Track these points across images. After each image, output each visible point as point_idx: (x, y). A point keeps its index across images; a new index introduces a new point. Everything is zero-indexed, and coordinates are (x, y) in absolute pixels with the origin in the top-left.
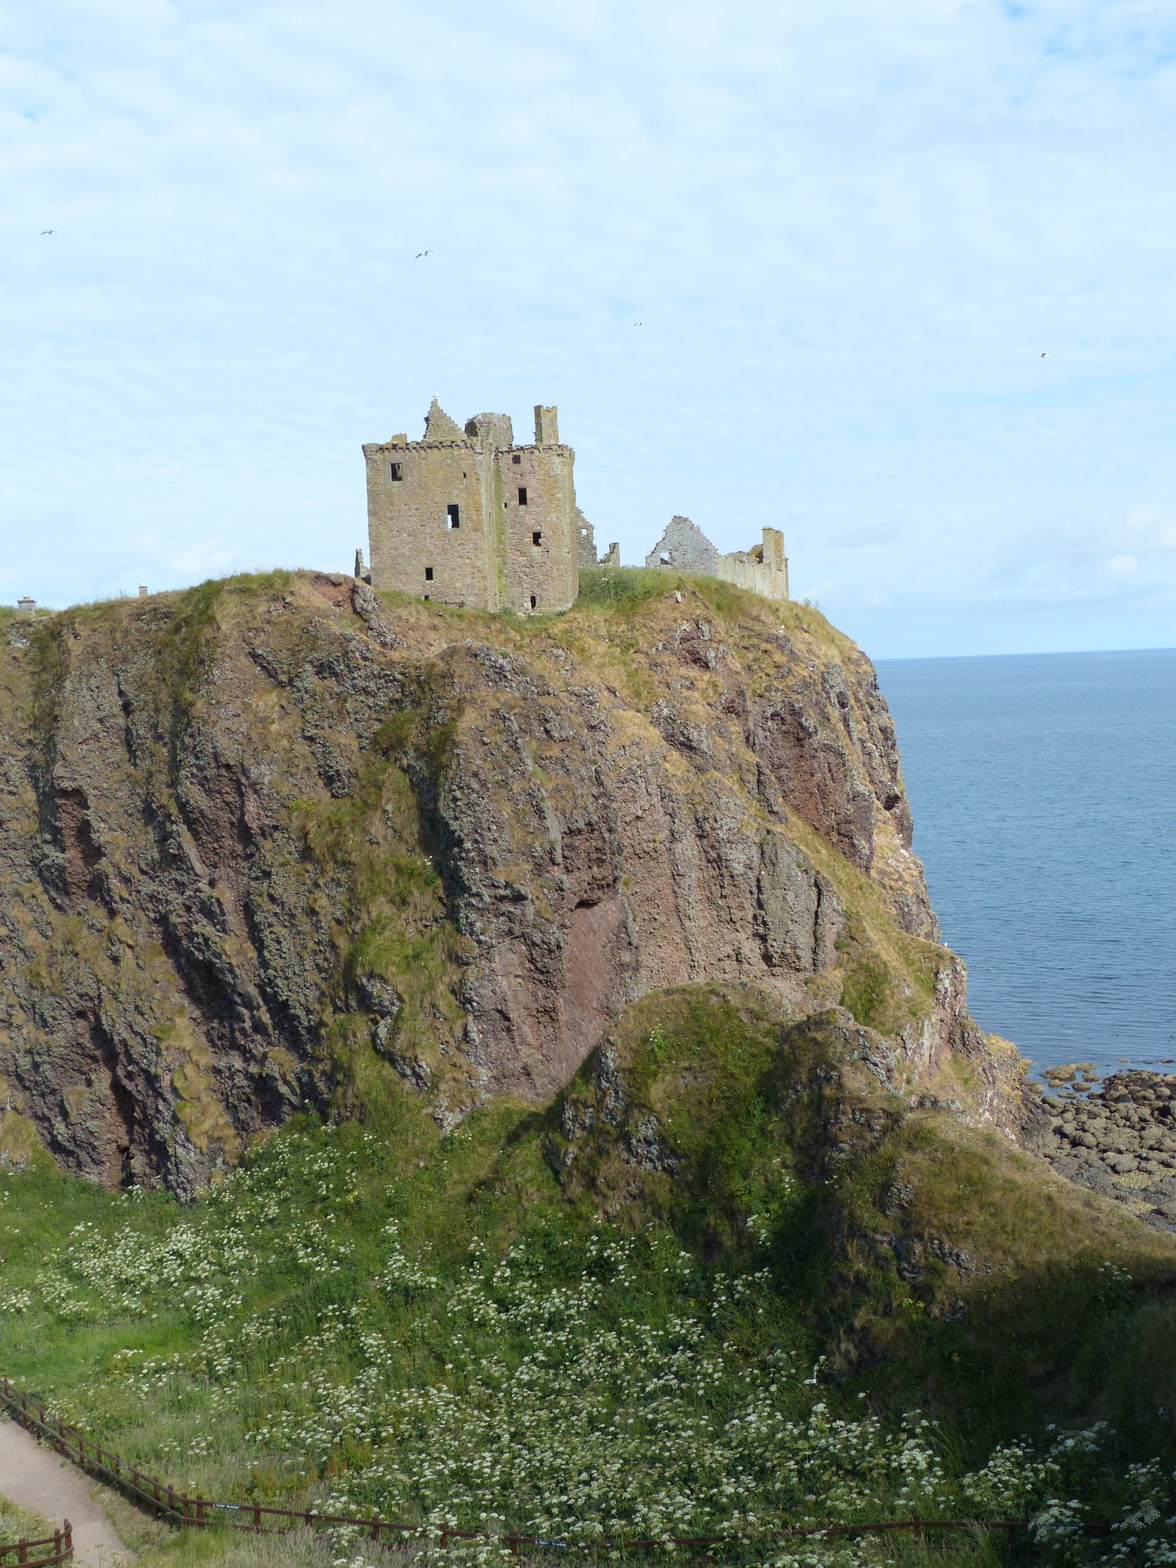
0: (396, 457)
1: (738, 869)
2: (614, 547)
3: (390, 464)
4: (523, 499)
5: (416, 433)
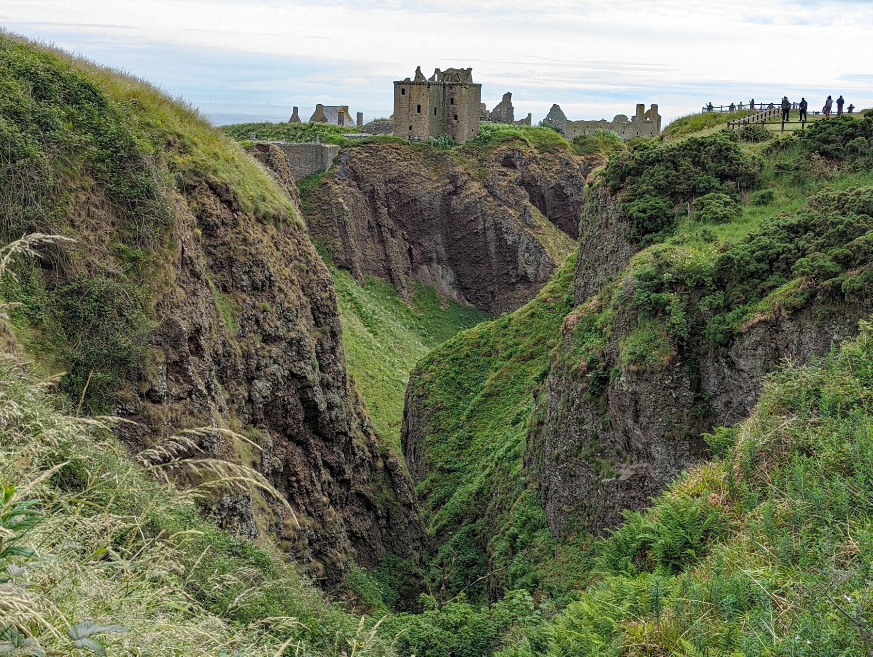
0: (404, 87)
1: (509, 243)
2: (530, 115)
3: (402, 88)
4: (452, 103)
5: (412, 80)
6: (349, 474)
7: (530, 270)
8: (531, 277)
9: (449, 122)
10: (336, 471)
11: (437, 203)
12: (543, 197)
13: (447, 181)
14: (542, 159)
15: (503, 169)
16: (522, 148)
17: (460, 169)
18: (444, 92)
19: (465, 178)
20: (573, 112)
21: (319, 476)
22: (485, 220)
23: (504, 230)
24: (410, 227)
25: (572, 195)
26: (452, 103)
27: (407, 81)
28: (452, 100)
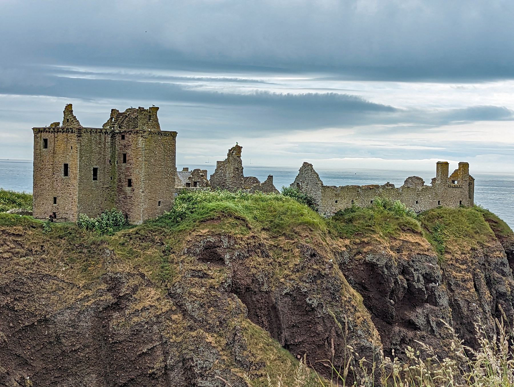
4: (125, 161)
9: (120, 190)
11: (86, 324)
12: (274, 308)
13: (104, 287)
14: (271, 247)
15: (202, 267)
16: (236, 231)
17: (124, 268)
18: (113, 144)
19: (133, 282)
22: (166, 354)
23: (197, 371)
24: (38, 365)
25: (320, 305)
26: (125, 161)
27: (55, 129)
28: (125, 155)
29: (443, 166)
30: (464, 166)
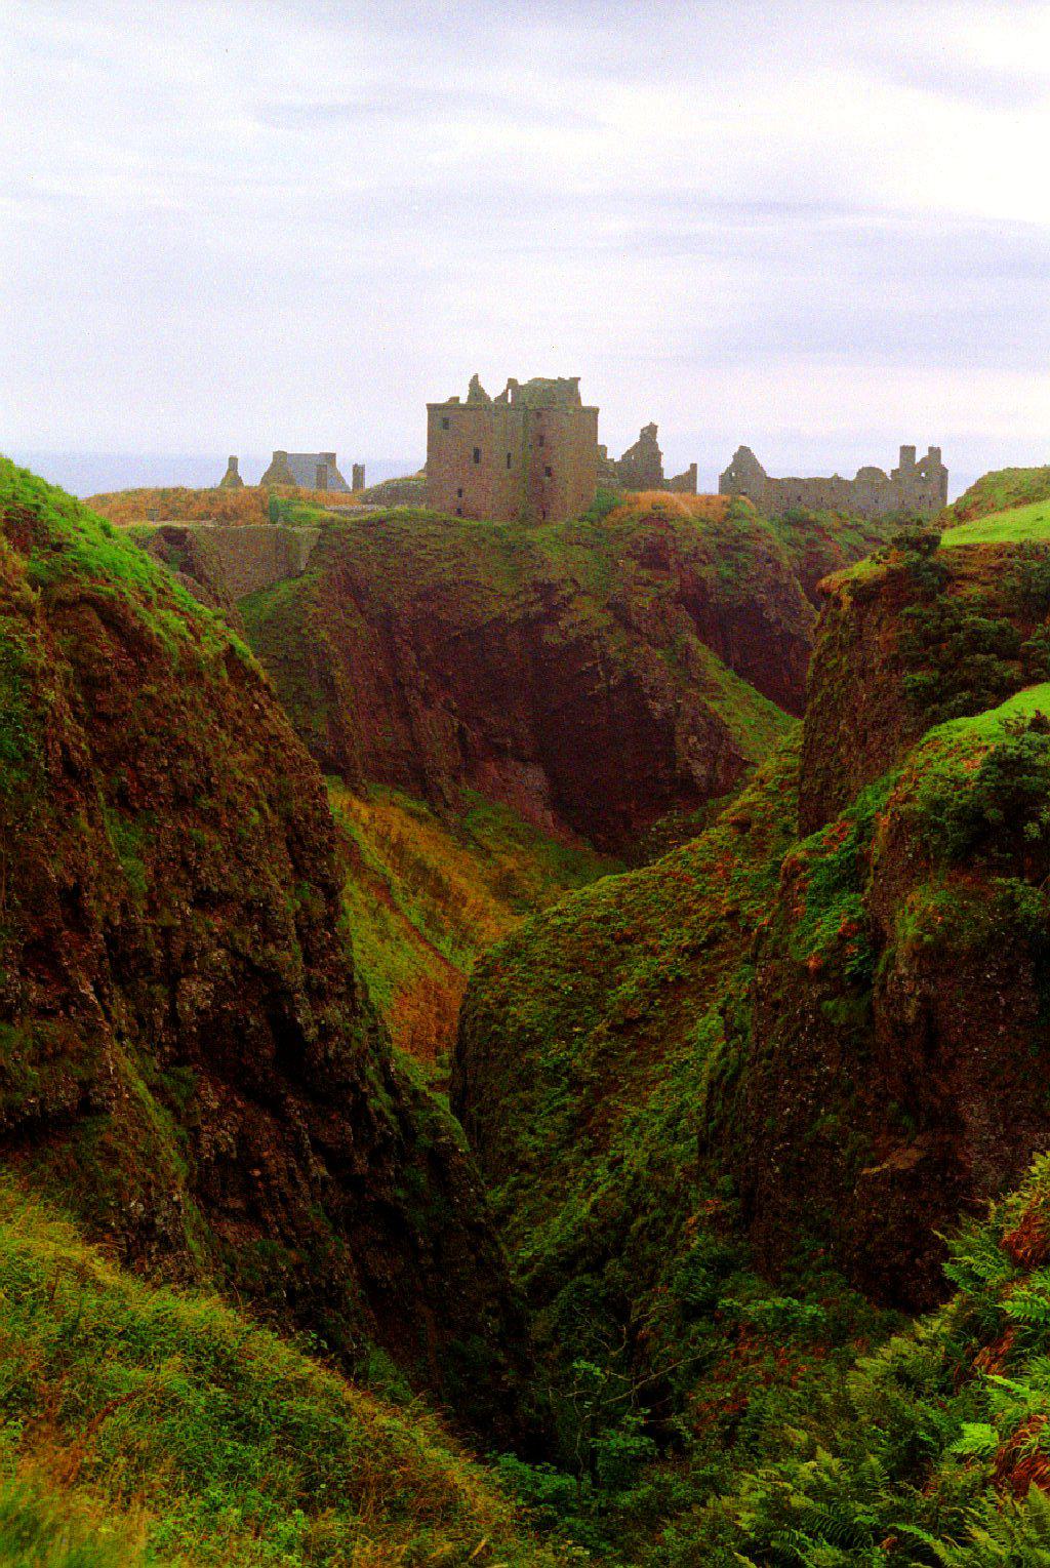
0: (446, 414)
2: (694, 467)
3: (443, 418)
5: (463, 400)
6: (361, 1164)
7: (700, 770)
8: (702, 784)
10: (337, 1160)
19: (569, 590)
20: (777, 464)
21: (306, 1169)
22: (609, 672)
25: (778, 622)
29: (907, 452)
30: (935, 452)
